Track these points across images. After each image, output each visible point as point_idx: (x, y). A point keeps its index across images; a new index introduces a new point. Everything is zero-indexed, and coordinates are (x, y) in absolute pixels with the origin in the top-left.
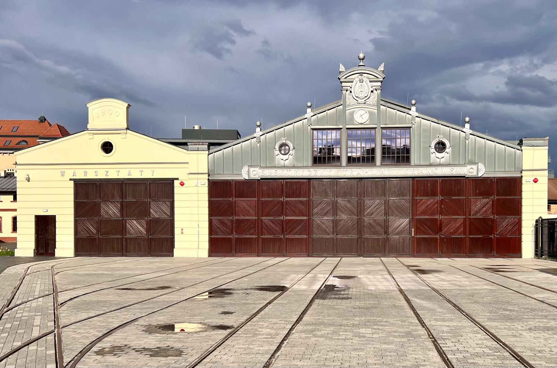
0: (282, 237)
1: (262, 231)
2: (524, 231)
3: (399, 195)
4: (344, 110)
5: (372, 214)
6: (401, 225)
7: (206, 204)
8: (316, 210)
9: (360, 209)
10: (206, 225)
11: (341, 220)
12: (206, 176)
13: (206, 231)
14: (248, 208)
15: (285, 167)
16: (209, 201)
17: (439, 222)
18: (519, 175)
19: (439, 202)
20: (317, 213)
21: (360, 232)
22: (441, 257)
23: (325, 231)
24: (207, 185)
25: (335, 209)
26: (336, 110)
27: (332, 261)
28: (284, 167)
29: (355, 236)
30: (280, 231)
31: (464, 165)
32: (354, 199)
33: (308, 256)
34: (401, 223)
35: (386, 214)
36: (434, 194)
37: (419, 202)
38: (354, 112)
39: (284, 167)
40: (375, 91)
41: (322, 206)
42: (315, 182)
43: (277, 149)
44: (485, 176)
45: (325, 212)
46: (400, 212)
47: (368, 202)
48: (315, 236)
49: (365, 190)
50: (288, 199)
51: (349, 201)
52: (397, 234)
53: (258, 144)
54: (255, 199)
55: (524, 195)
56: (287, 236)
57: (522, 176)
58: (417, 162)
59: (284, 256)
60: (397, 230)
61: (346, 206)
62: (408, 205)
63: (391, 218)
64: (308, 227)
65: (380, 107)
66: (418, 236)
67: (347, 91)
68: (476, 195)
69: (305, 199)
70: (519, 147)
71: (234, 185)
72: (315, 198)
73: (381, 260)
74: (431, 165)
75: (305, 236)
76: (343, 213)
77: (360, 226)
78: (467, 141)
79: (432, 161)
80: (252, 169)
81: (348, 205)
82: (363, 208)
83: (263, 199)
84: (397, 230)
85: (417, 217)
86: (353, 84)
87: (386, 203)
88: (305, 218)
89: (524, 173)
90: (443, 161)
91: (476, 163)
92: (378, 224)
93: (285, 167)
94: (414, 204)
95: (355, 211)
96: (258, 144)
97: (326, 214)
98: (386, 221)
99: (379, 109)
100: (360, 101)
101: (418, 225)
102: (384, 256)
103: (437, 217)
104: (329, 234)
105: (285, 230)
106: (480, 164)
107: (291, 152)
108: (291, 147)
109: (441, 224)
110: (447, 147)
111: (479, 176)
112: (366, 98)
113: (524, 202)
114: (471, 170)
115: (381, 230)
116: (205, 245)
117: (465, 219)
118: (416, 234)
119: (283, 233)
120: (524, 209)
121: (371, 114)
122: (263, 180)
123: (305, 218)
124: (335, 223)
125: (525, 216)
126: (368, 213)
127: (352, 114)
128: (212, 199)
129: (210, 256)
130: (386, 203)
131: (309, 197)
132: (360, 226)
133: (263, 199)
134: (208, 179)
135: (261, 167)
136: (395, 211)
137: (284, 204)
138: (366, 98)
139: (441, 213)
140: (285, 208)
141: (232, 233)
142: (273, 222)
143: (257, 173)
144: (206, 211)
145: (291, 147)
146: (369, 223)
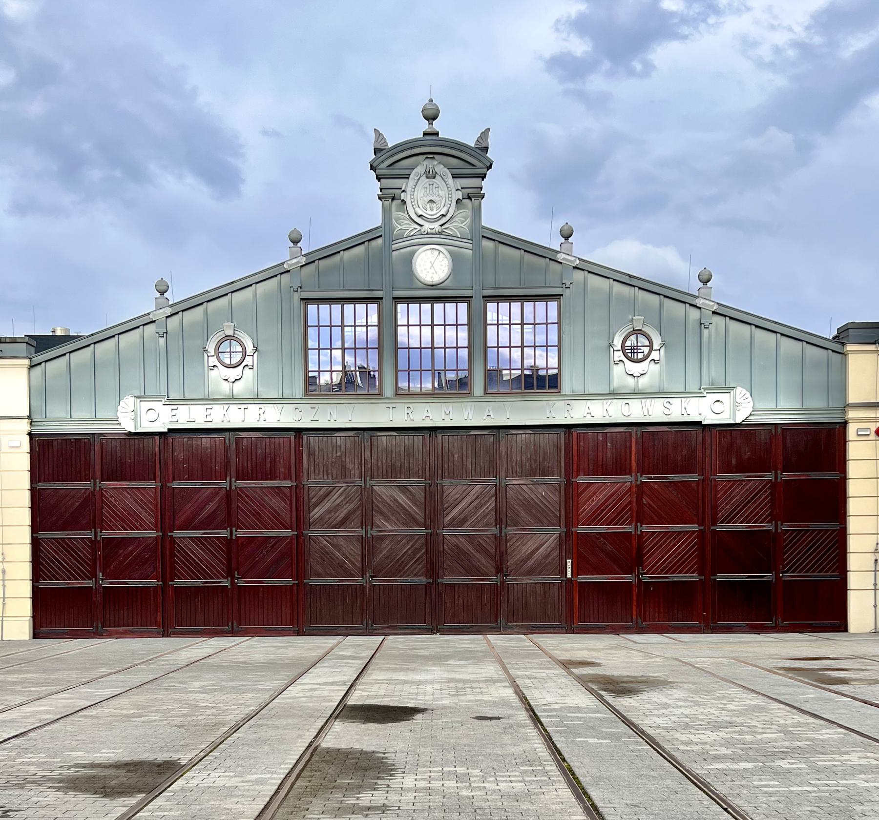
0: (225, 582)
1: (173, 568)
2: (854, 562)
3: (532, 473)
4: (388, 248)
5: (464, 521)
6: (537, 549)
7: (25, 498)
8: (317, 513)
9: (434, 507)
10: (25, 553)
11: (382, 538)
12: (25, 426)
13: (25, 571)
14: (135, 507)
15: (233, 399)
16: (33, 490)
17: (635, 542)
18: (836, 418)
19: (635, 489)
20: (321, 518)
21: (433, 570)
22: (641, 631)
23: (341, 565)
24: (26, 447)
25: (367, 509)
26: (367, 249)
27: (360, 645)
28: (232, 399)
29: (422, 580)
30: (221, 568)
31: (698, 394)
32: (416, 484)
33: (299, 633)
34: (539, 542)
35: (499, 521)
36: (620, 467)
37: (584, 491)
38: (413, 253)
39: (232, 399)
40: (467, 201)
41: (335, 498)
42: (314, 440)
43: (211, 350)
44: (753, 420)
45: (339, 519)
46: (534, 516)
47: (452, 489)
48: (314, 581)
49: (446, 459)
50: (241, 484)
51: (403, 489)
52: (530, 572)
53: (162, 341)
54: (151, 484)
55: (853, 469)
56: (242, 582)
57: (845, 423)
58: (579, 388)
59: (233, 633)
60: (531, 562)
61: (396, 500)
62: (556, 499)
63: (510, 531)
64: (295, 556)
65: (480, 244)
66: (584, 578)
67: (393, 199)
68: (728, 469)
69: (287, 483)
70: (837, 347)
71: (97, 448)
72: (313, 481)
73: (488, 641)
74: (613, 394)
75: (288, 581)
76: (387, 519)
77: (433, 554)
78: (705, 332)
79: (616, 383)
80: (145, 405)
81: (402, 499)
82: (440, 507)
83: (176, 484)
84: (531, 562)
85: (582, 529)
86: (411, 182)
87: (500, 492)
88: (287, 533)
89: (852, 414)
90: (643, 382)
91: (728, 389)
92: (480, 548)
93: (233, 399)
94: (571, 494)
95: (420, 517)
96: (162, 341)
97: (343, 523)
98: (498, 540)
99: (477, 247)
100: (427, 226)
101: (582, 550)
102: (497, 630)
103: (628, 528)
104: (352, 575)
105: (234, 565)
106: (739, 389)
107: (248, 361)
108: (250, 349)
109: (640, 548)
110: (656, 346)
111: (738, 421)
112: (444, 220)
113: (853, 488)
114: (718, 407)
115: (483, 561)
116: (25, 608)
117: (701, 533)
118: (576, 572)
119: (230, 574)
120: (854, 506)
121: (456, 259)
122: (175, 436)
123: (287, 533)
124: (369, 546)
125: (854, 525)
126: (454, 519)
127: (409, 260)
128: (42, 485)
129: (36, 635)
130: (500, 492)
131: (298, 477)
132: (433, 554)
133: (176, 484)
134: (30, 434)
135: (171, 401)
136: (523, 513)
137: (234, 496)
138: (444, 220)
139: (640, 518)
140: (234, 506)
141: (93, 575)
142: (203, 544)
143: (157, 418)
144: (25, 516)
145: (250, 349)
146: (457, 546)
